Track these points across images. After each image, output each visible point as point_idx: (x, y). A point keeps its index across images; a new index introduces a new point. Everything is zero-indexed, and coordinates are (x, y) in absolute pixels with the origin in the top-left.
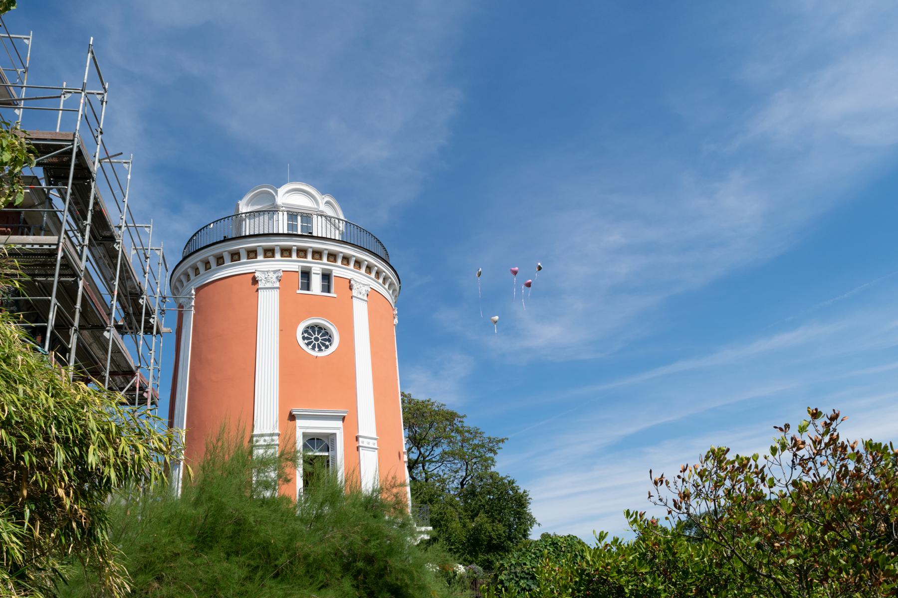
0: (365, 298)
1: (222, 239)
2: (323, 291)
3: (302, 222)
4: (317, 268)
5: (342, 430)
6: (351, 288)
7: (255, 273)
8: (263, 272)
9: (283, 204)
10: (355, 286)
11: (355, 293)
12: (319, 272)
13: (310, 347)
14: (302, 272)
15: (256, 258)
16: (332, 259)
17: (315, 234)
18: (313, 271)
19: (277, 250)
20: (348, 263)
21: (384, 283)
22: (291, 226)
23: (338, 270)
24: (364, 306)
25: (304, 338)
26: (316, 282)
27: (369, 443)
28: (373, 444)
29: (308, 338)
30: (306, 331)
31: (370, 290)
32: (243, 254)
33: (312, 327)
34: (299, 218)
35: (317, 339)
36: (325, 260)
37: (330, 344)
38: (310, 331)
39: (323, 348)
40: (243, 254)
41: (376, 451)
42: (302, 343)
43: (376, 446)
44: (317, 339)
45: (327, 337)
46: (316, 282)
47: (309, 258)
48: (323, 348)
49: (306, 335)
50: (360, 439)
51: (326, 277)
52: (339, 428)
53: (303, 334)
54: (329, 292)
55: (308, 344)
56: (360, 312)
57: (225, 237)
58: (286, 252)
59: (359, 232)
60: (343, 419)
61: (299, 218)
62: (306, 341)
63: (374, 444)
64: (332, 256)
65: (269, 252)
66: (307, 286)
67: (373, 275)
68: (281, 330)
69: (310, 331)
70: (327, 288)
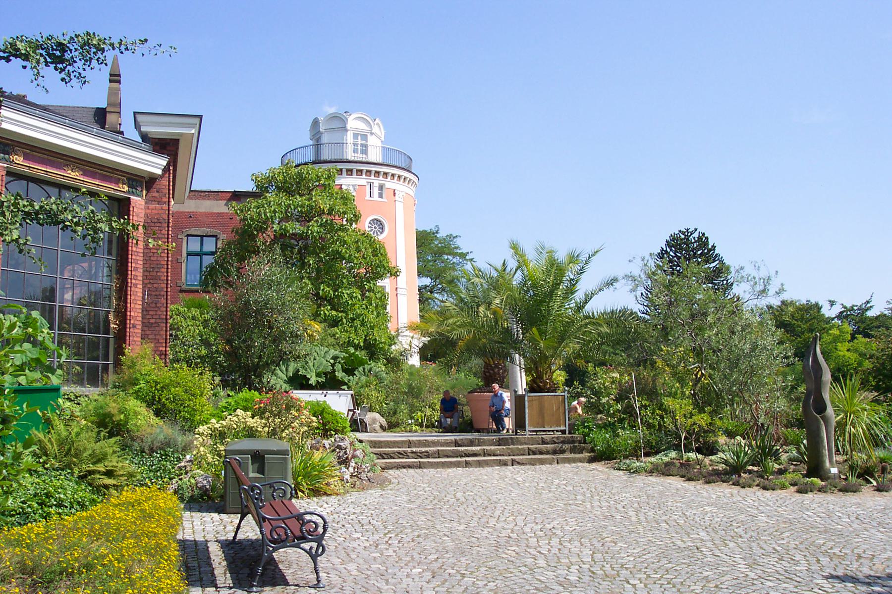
4: (376, 183)
5: (389, 284)
6: (394, 194)
7: (341, 185)
8: (346, 185)
10: (396, 195)
11: (397, 197)
16: (385, 176)
20: (393, 179)
23: (390, 184)
26: (376, 191)
31: (405, 194)
33: (373, 220)
34: (359, 137)
35: (375, 228)
36: (381, 178)
38: (372, 222)
39: (379, 233)
44: (375, 228)
45: (382, 229)
47: (372, 177)
50: (398, 289)
51: (381, 187)
54: (382, 198)
56: (400, 207)
58: (359, 172)
61: (359, 137)
65: (350, 172)
69: (372, 222)
70: (381, 196)
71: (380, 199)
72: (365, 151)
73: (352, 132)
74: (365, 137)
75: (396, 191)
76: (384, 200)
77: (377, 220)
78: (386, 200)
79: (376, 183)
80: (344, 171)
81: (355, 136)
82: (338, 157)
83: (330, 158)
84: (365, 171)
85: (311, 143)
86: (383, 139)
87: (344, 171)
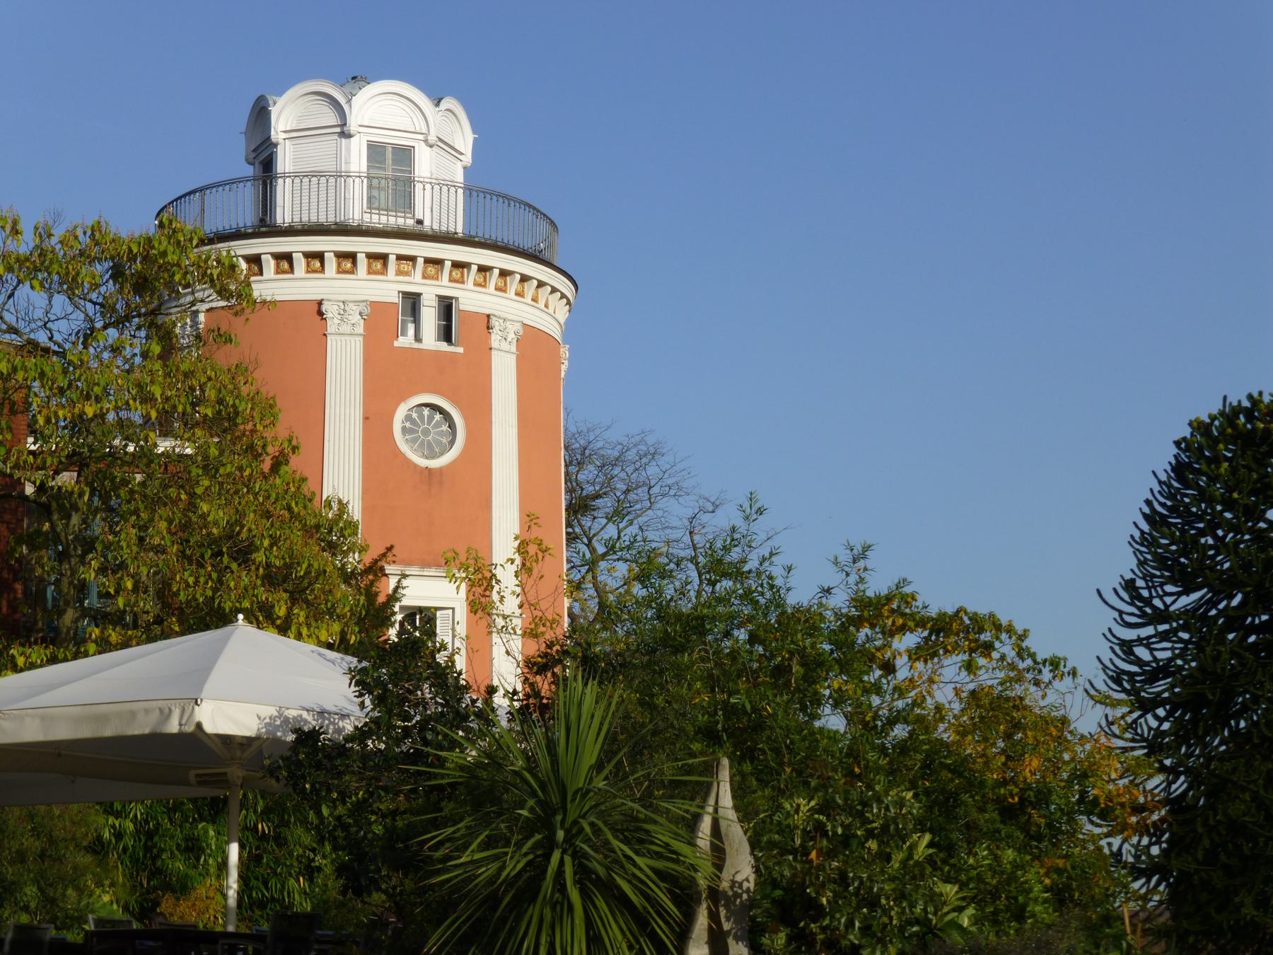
4: (430, 293)
25: (404, 430)
29: (411, 431)
32: (300, 262)
40: (300, 262)
51: (446, 307)
68: (366, 418)
70: (446, 334)
71: (443, 346)
72: (405, 200)
73: (364, 140)
74: (404, 155)
75: (494, 321)
78: (460, 350)
80: (330, 260)
81: (375, 151)
82: (325, 216)
83: (297, 219)
85: (249, 171)
86: (468, 159)
87: (330, 260)
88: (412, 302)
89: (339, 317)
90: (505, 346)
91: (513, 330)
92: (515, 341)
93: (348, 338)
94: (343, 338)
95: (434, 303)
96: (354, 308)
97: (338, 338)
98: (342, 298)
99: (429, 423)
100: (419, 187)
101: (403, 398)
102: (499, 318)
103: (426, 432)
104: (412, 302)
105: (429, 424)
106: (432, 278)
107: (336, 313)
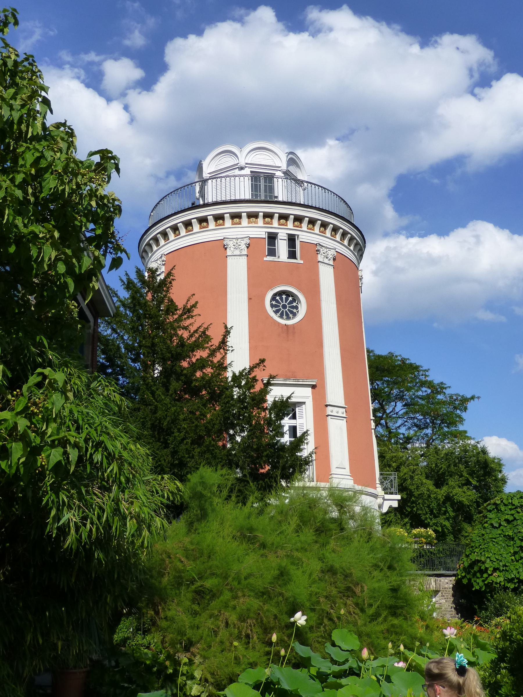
0: (331, 262)
1: (190, 206)
2: (288, 258)
3: (265, 182)
4: (282, 234)
5: (311, 398)
9: (246, 164)
12: (285, 238)
13: (279, 314)
14: (269, 237)
15: (224, 225)
17: (280, 199)
18: (280, 236)
19: (244, 215)
21: (349, 245)
22: (255, 188)
24: (331, 269)
25: (272, 306)
26: (282, 247)
27: (338, 412)
28: (341, 412)
29: (276, 306)
30: (273, 298)
31: (335, 254)
35: (284, 307)
37: (298, 312)
38: (278, 298)
39: (291, 316)
41: (345, 419)
42: (270, 311)
43: (344, 415)
46: (282, 247)
48: (291, 316)
49: (274, 303)
52: (307, 397)
53: (271, 301)
55: (276, 312)
57: (193, 204)
59: (324, 193)
60: (313, 387)
62: (274, 309)
63: (343, 413)
64: (298, 219)
66: (272, 252)
67: (338, 237)
68: (250, 299)
69: (278, 298)
70: (292, 255)
76: (299, 261)
77: (288, 294)
78: (302, 262)
79: (282, 234)
84: (261, 214)
88: (272, 238)
89: (234, 247)
90: (326, 261)
91: (331, 253)
92: (332, 259)
93: (238, 257)
94: (236, 257)
95: (286, 238)
96: (242, 241)
97: (233, 257)
98: (235, 237)
99: (286, 302)
100: (275, 180)
101: (271, 288)
102: (322, 246)
103: (284, 307)
104: (272, 238)
105: (286, 302)
106: (283, 225)
107: (232, 245)
